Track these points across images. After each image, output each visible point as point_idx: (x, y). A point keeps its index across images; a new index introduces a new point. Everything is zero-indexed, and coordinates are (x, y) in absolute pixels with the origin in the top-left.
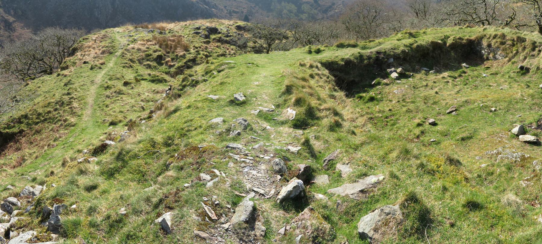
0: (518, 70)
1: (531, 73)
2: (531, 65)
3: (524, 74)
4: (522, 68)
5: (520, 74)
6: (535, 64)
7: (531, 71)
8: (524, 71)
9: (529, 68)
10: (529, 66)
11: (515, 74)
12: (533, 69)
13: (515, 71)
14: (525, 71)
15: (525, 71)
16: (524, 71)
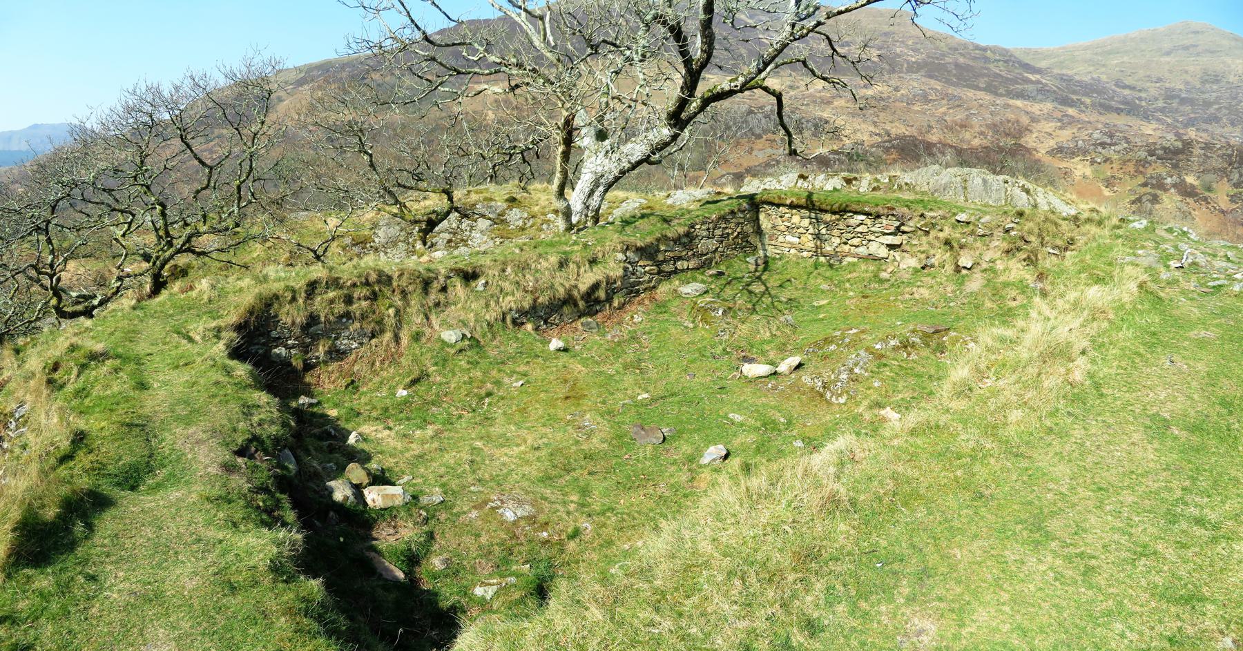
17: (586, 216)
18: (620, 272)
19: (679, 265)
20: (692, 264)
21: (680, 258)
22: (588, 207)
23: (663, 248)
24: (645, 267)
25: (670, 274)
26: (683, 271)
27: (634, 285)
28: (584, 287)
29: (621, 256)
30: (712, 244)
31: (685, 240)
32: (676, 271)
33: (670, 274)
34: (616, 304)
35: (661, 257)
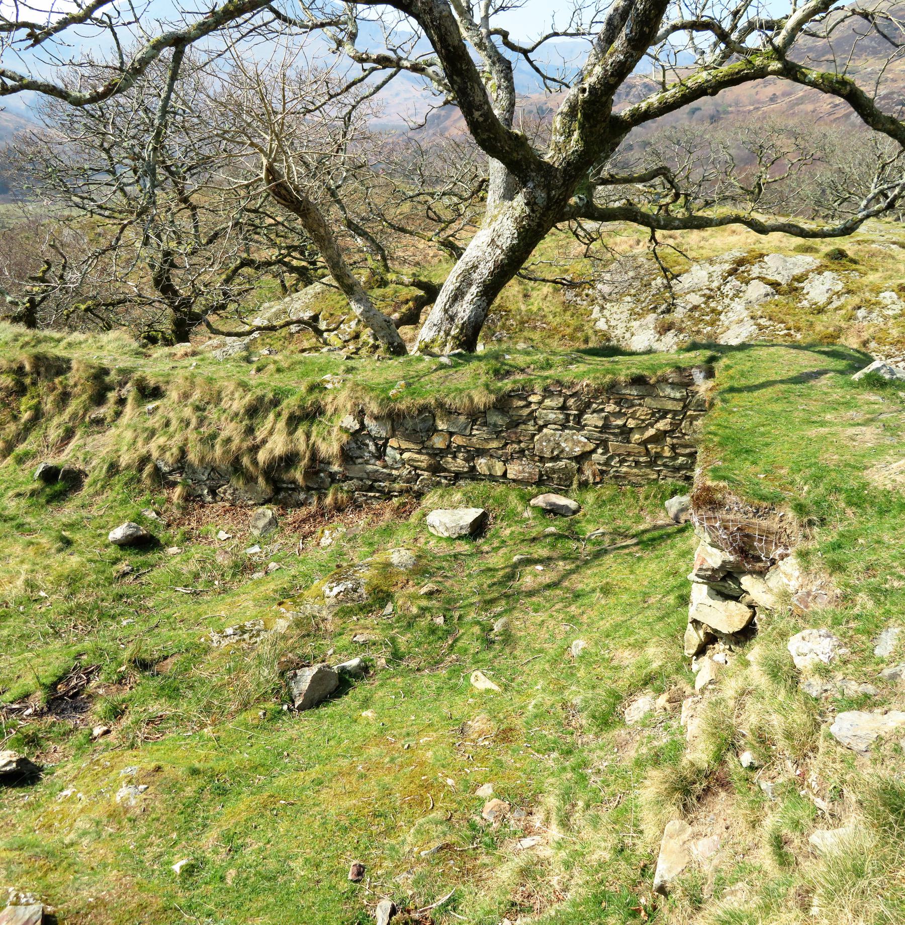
0: (37, 485)
1: (87, 489)
2: (86, 462)
3: (59, 497)
4: (50, 475)
5: (42, 500)
6: (103, 452)
7: (87, 481)
8: (58, 486)
9: (81, 472)
10: (80, 466)
11: (24, 502)
12: (96, 471)
13: (22, 489)
14: (60, 483)
15: (60, 483)
16: (58, 486)
17: (447, 334)
18: (335, 448)
19: (482, 464)
20: (514, 470)
21: (481, 452)
22: (452, 319)
23: (441, 426)
24: (402, 454)
25: (458, 476)
26: (492, 478)
27: (375, 478)
28: (262, 456)
29: (351, 423)
30: (575, 442)
31: (497, 419)
32: (473, 475)
33: (458, 476)
34: (329, 500)
35: (438, 442)
